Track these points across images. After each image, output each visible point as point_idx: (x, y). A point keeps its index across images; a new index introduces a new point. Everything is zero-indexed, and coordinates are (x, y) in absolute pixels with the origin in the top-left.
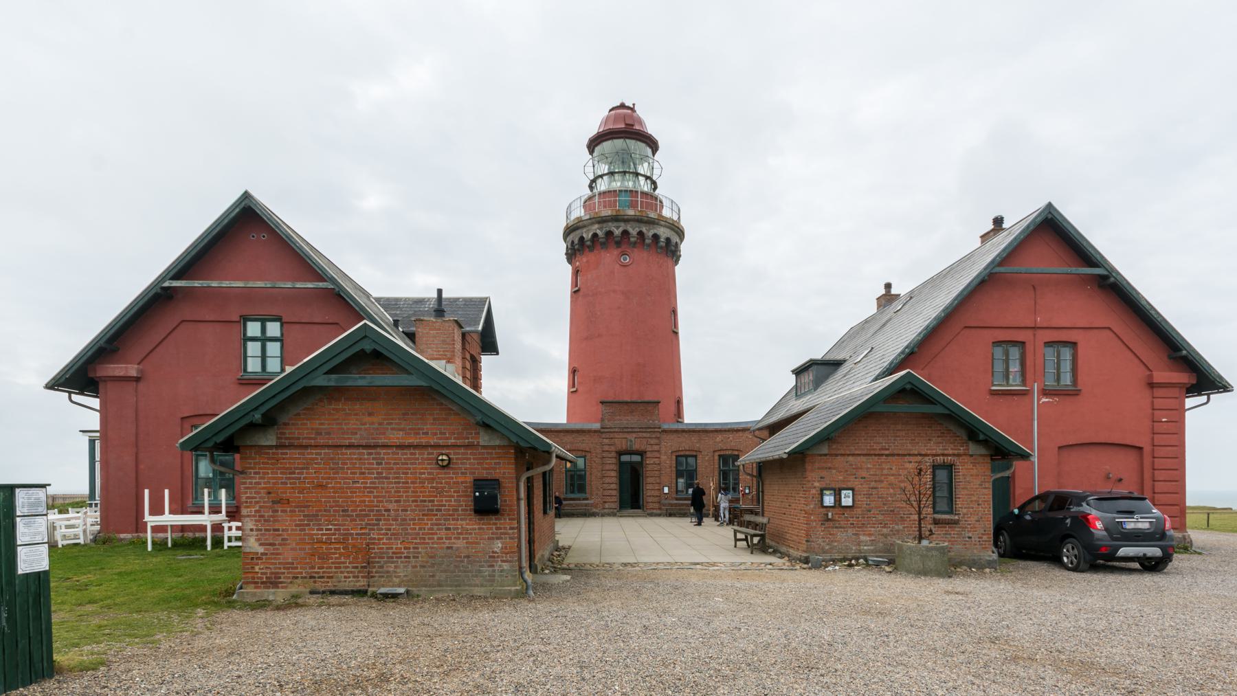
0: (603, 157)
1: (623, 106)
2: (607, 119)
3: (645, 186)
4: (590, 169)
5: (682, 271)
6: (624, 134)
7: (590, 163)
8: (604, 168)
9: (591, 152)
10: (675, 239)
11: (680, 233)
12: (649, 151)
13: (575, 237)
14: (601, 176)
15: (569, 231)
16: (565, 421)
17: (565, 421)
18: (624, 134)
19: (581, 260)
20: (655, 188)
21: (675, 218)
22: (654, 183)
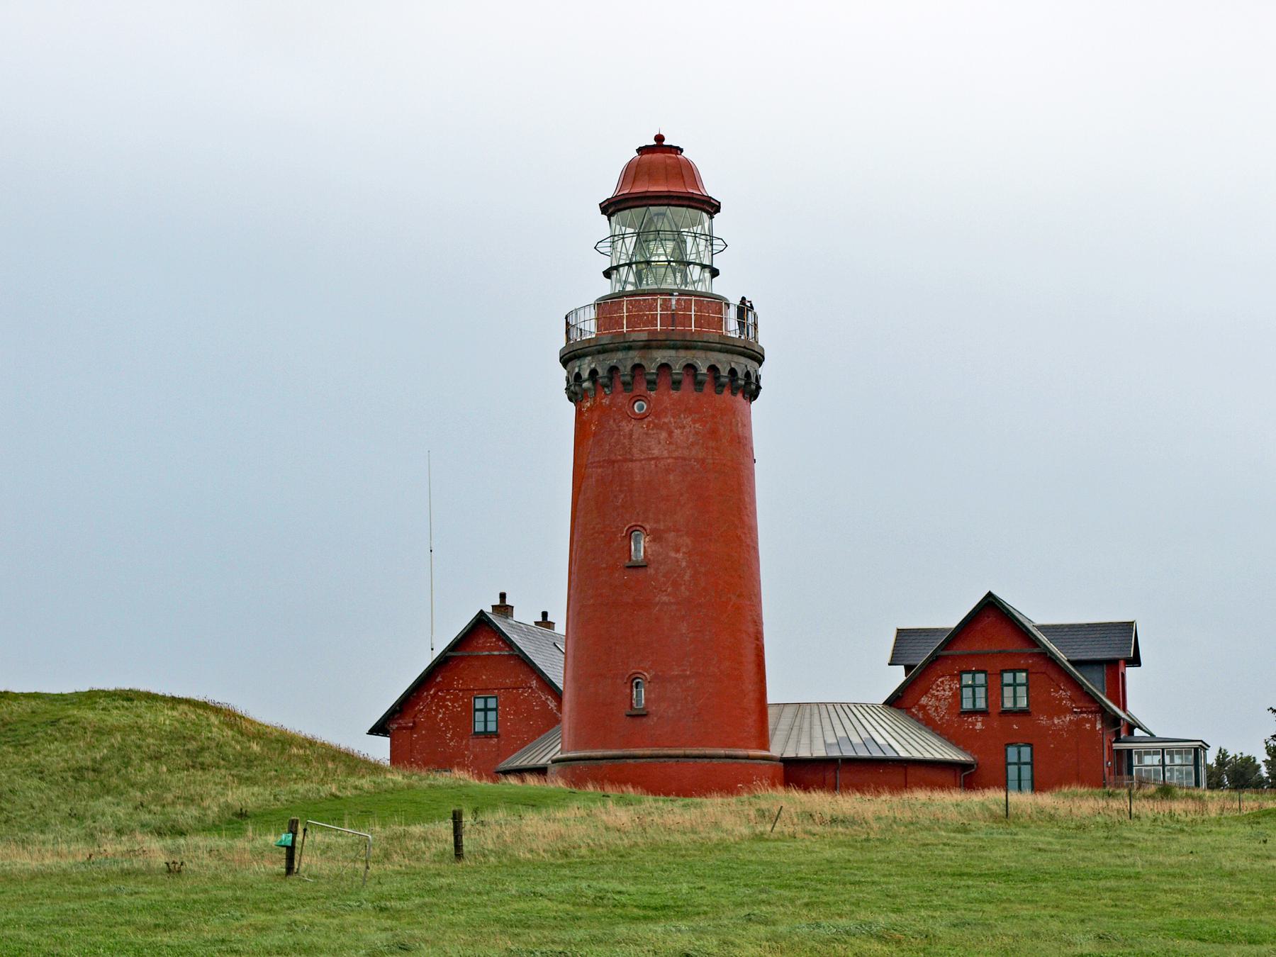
6: (659, 187)
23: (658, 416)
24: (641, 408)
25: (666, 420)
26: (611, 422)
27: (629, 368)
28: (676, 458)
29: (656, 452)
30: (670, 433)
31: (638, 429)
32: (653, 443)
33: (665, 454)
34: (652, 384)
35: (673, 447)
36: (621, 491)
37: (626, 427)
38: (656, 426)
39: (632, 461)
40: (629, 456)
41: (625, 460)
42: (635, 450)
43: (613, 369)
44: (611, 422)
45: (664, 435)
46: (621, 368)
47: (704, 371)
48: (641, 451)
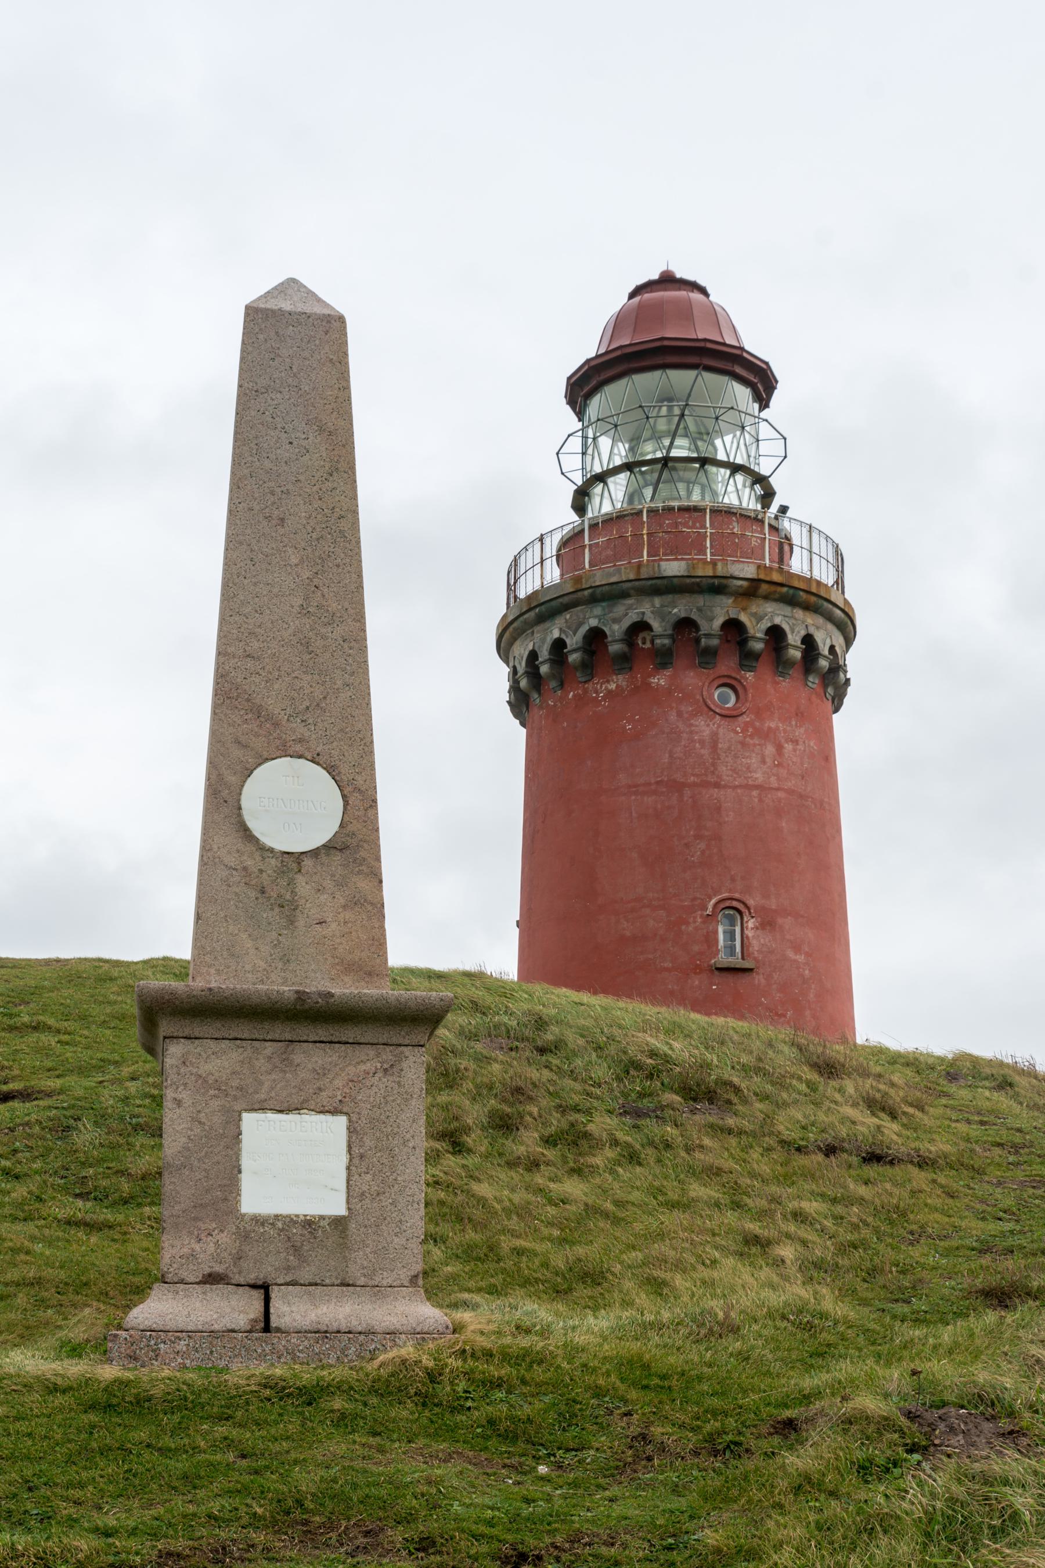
0: (612, 426)
1: (667, 280)
2: (619, 322)
3: (736, 494)
4: (573, 462)
5: (847, 726)
7: (576, 444)
8: (611, 451)
9: (580, 415)
10: (826, 637)
11: (846, 625)
12: (742, 394)
13: (521, 650)
14: (601, 478)
15: (504, 646)
16: (181, 947)
17: (181, 947)
18: (666, 354)
19: (537, 714)
20: (768, 496)
21: (825, 575)
22: (759, 479)
23: (758, 713)
24: (724, 699)
25: (773, 725)
26: (673, 716)
27: (718, 623)
28: (791, 792)
29: (759, 776)
30: (779, 748)
31: (727, 734)
32: (754, 761)
33: (774, 782)
34: (748, 658)
35: (783, 772)
36: (698, 837)
37: (704, 727)
38: (758, 732)
39: (717, 785)
40: (711, 779)
41: (706, 784)
42: (723, 769)
43: (685, 625)
44: (673, 716)
45: (770, 750)
46: (701, 622)
47: (826, 652)
48: (734, 770)
